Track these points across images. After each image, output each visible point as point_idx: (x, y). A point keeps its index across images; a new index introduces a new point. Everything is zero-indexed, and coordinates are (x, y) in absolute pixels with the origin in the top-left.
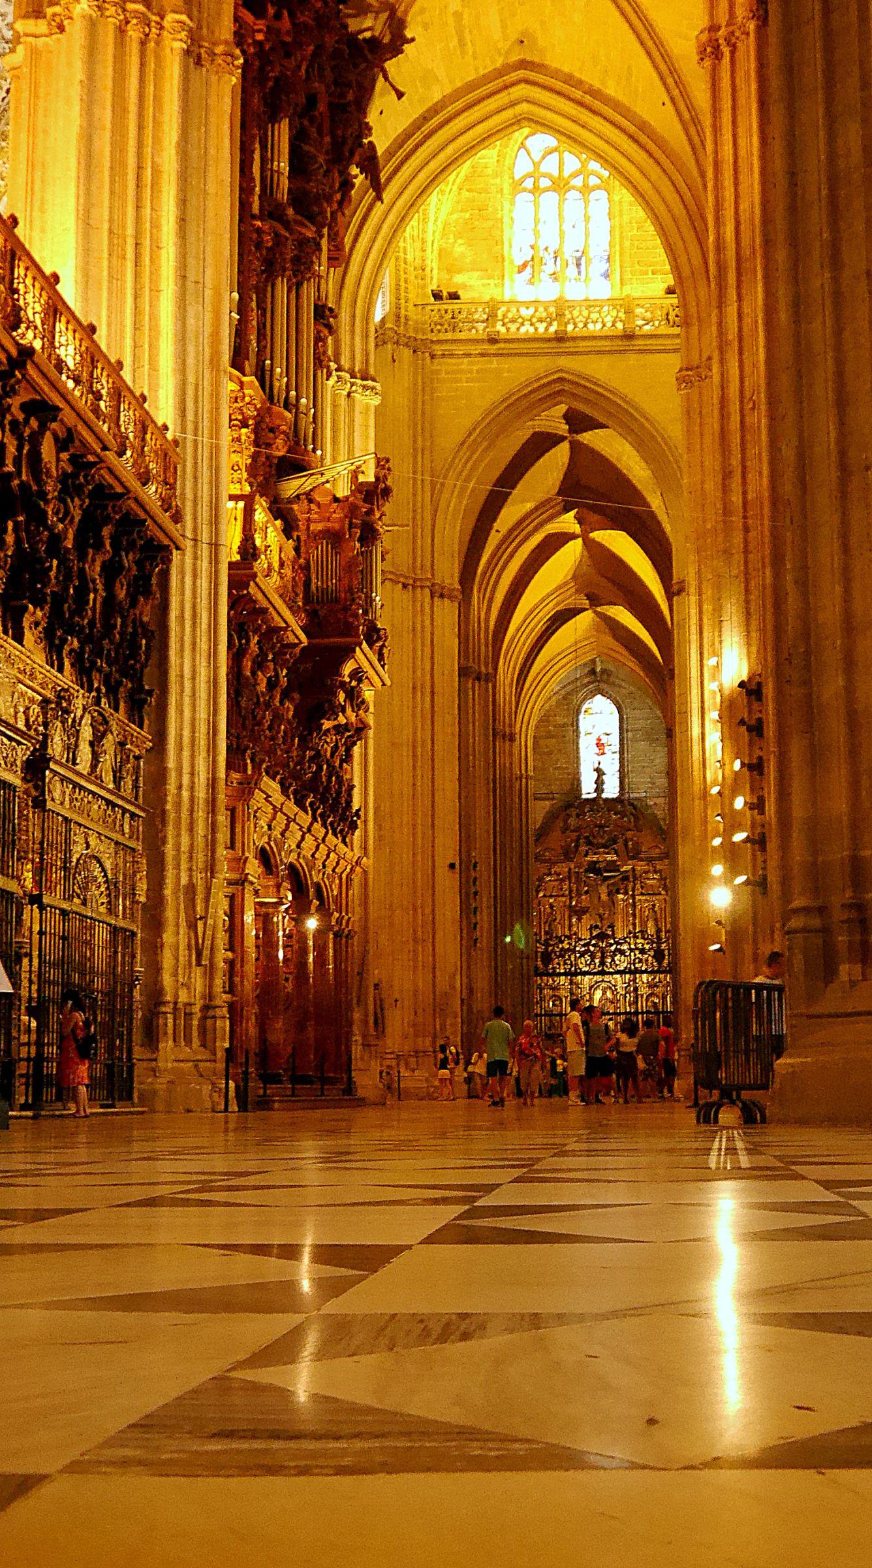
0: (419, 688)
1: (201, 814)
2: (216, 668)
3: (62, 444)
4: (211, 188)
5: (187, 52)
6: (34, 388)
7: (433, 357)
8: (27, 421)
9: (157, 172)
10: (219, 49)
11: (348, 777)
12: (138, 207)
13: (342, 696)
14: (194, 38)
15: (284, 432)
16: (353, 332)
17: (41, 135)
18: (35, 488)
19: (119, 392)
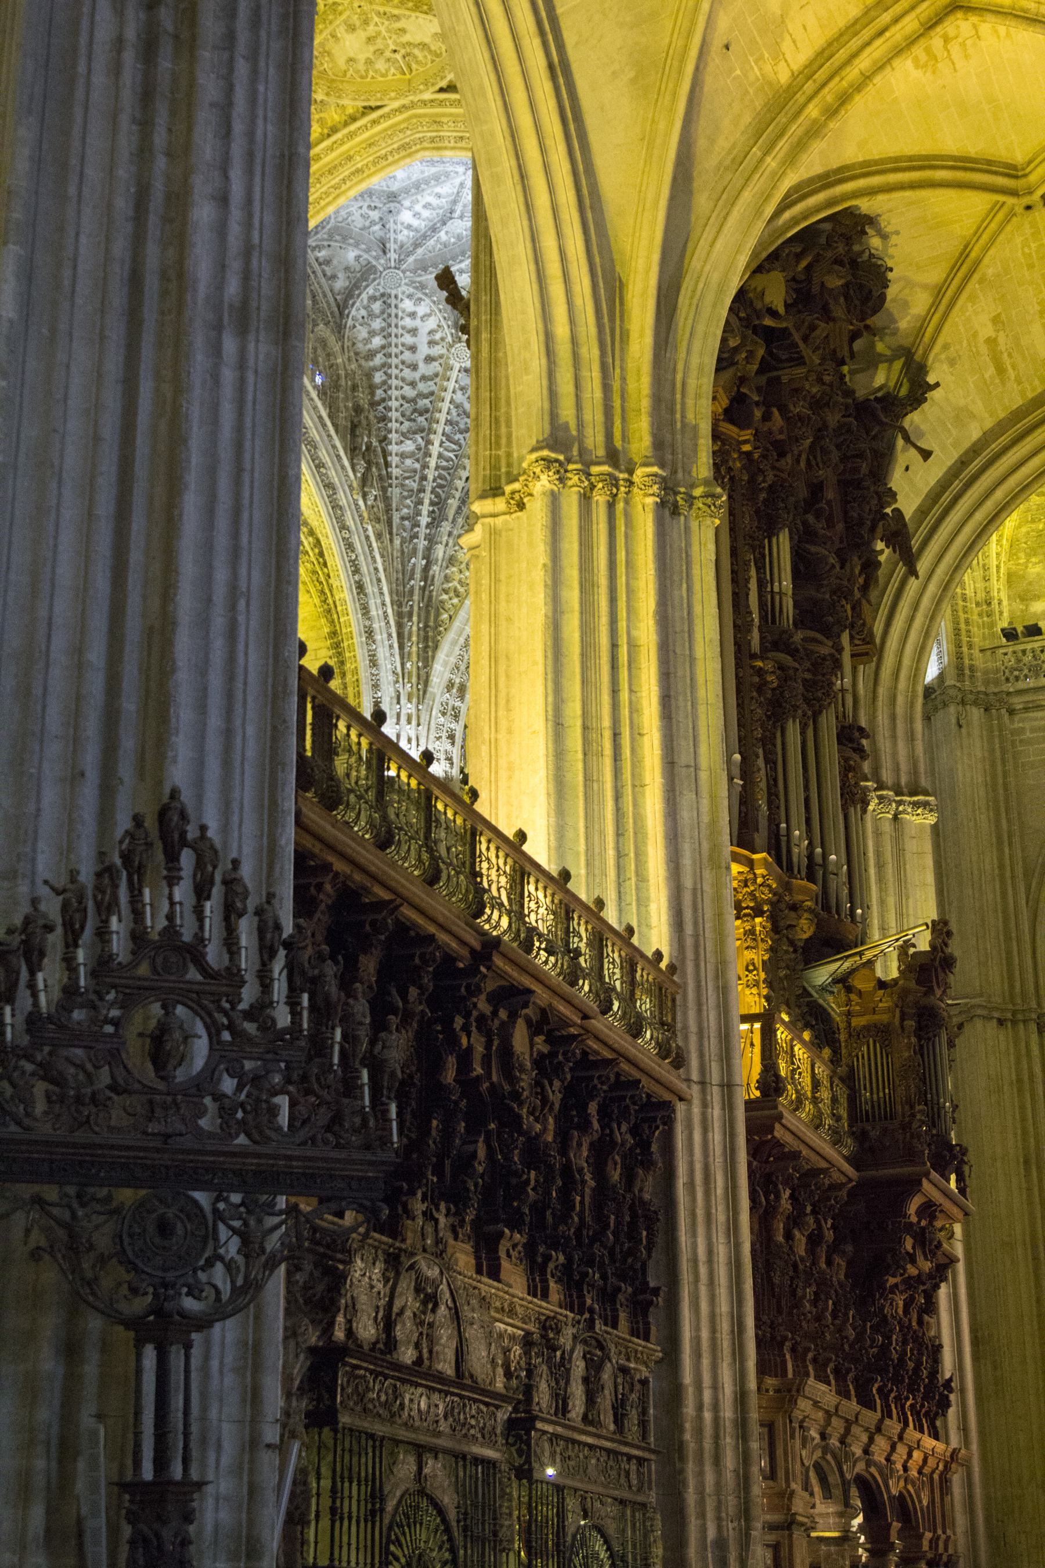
0: (1033, 1161)
1: (728, 1440)
2: (737, 1246)
3: (535, 1028)
4: (699, 651)
5: (661, 505)
6: (501, 975)
7: (1011, 712)
8: (495, 1013)
9: (633, 646)
10: (698, 492)
11: (932, 1333)
12: (615, 692)
13: (909, 1244)
14: (668, 487)
15: (810, 910)
16: (894, 737)
17: (503, 623)
18: (507, 1087)
19: (600, 936)
